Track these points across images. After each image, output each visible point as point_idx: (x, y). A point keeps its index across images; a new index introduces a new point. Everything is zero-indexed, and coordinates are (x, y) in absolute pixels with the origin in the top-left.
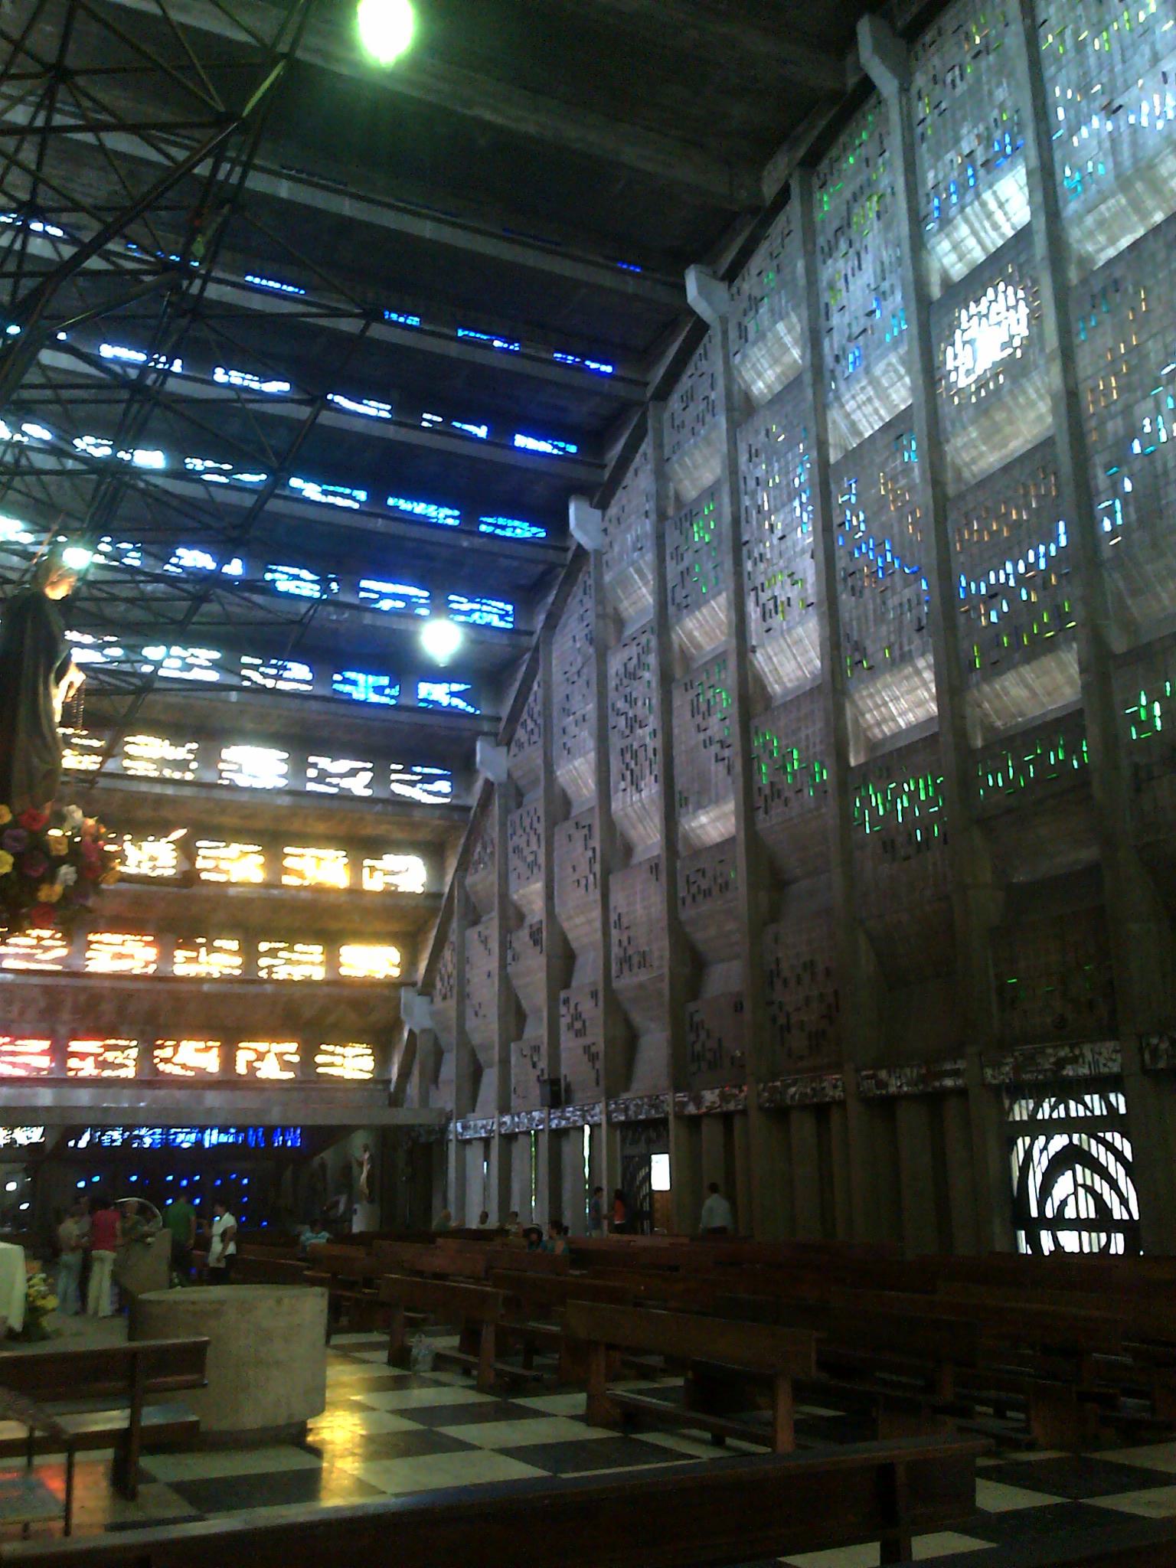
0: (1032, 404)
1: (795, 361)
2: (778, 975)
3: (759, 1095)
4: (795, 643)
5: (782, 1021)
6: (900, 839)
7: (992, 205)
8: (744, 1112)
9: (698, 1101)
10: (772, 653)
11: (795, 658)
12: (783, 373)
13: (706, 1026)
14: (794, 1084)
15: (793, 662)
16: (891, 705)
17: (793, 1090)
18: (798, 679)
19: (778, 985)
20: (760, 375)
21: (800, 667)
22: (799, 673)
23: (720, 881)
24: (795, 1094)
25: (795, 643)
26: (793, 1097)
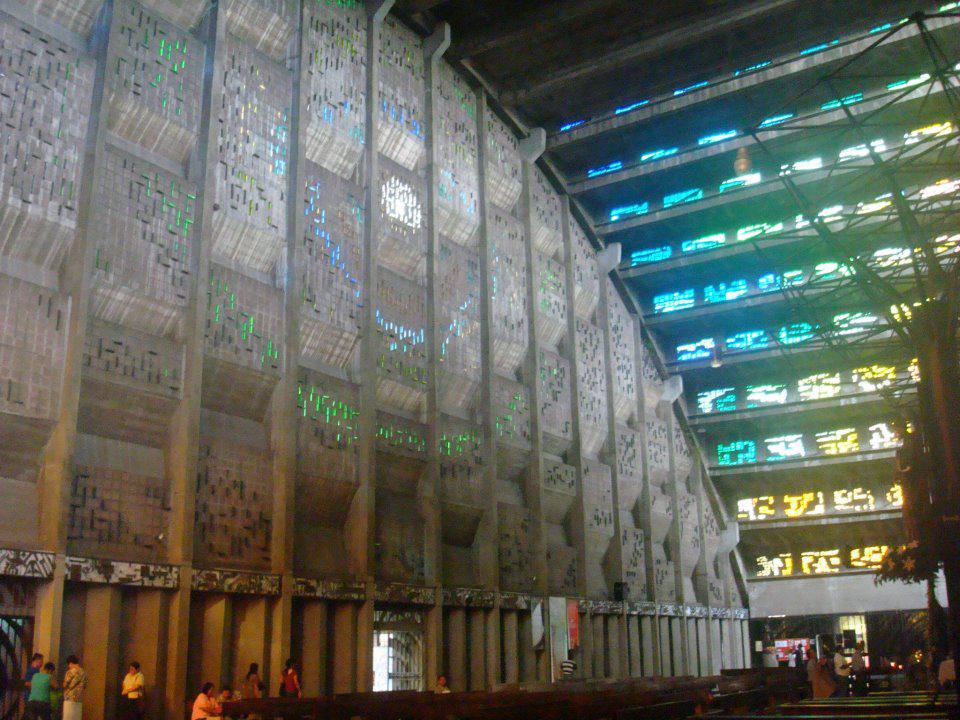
0: (407, 256)
1: (259, 38)
2: (207, 482)
3: (193, 578)
4: (248, 236)
5: (204, 518)
6: (327, 433)
7: (401, 141)
8: (169, 593)
9: (106, 569)
10: (226, 223)
11: (238, 243)
12: (246, 31)
13: (98, 495)
14: (234, 575)
15: (233, 243)
16: (310, 339)
17: (230, 581)
18: (224, 253)
19: (205, 489)
20: (235, 9)
21: (234, 249)
22: (230, 252)
23: (147, 369)
24: (233, 583)
25: (248, 236)
26: (230, 586)
